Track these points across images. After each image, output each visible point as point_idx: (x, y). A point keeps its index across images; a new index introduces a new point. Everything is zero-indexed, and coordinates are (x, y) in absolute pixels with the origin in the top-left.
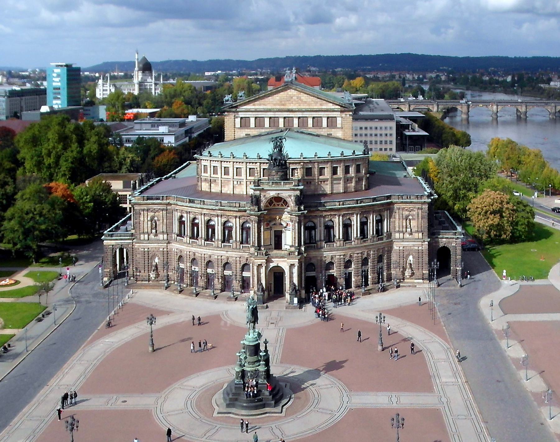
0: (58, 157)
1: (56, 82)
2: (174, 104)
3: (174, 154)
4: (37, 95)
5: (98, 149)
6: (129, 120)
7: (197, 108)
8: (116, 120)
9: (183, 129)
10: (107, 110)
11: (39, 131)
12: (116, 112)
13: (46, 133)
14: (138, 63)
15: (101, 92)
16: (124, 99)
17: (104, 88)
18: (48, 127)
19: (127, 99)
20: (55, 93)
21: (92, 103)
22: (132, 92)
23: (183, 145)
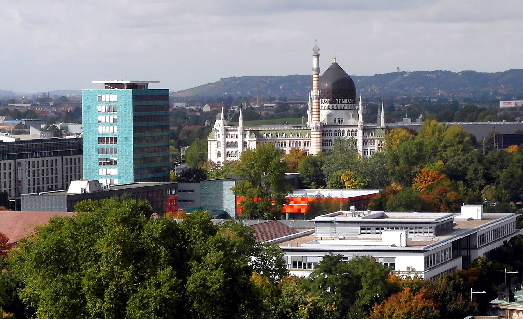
0: (122, 298)
1: (106, 124)
2: (418, 179)
3: (426, 297)
4: (56, 154)
5: (225, 283)
6: (295, 216)
7: (481, 188)
8: (261, 217)
9: (446, 239)
10: (238, 191)
11: (72, 236)
12: (263, 194)
13: (93, 242)
14: (319, 79)
15: (221, 150)
16: (284, 164)
17: (229, 140)
18: (95, 228)
19: (290, 165)
20: (103, 151)
21: (197, 174)
22: (302, 147)
23: (450, 276)
